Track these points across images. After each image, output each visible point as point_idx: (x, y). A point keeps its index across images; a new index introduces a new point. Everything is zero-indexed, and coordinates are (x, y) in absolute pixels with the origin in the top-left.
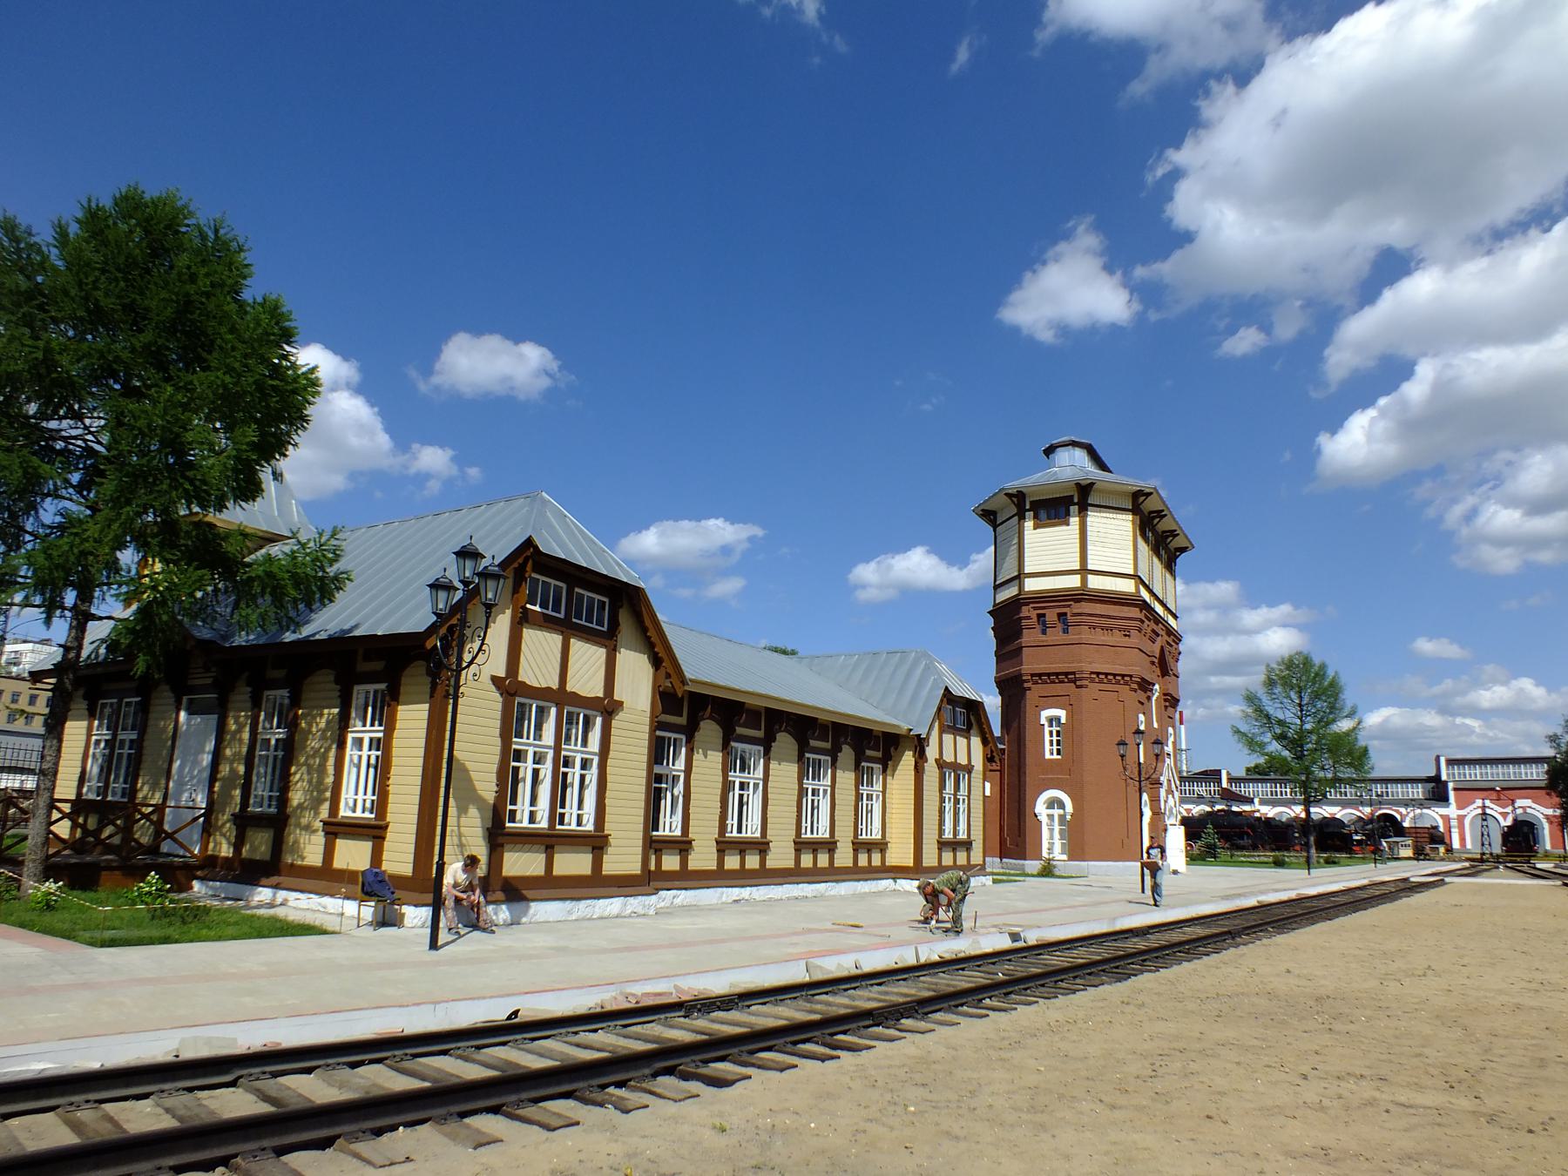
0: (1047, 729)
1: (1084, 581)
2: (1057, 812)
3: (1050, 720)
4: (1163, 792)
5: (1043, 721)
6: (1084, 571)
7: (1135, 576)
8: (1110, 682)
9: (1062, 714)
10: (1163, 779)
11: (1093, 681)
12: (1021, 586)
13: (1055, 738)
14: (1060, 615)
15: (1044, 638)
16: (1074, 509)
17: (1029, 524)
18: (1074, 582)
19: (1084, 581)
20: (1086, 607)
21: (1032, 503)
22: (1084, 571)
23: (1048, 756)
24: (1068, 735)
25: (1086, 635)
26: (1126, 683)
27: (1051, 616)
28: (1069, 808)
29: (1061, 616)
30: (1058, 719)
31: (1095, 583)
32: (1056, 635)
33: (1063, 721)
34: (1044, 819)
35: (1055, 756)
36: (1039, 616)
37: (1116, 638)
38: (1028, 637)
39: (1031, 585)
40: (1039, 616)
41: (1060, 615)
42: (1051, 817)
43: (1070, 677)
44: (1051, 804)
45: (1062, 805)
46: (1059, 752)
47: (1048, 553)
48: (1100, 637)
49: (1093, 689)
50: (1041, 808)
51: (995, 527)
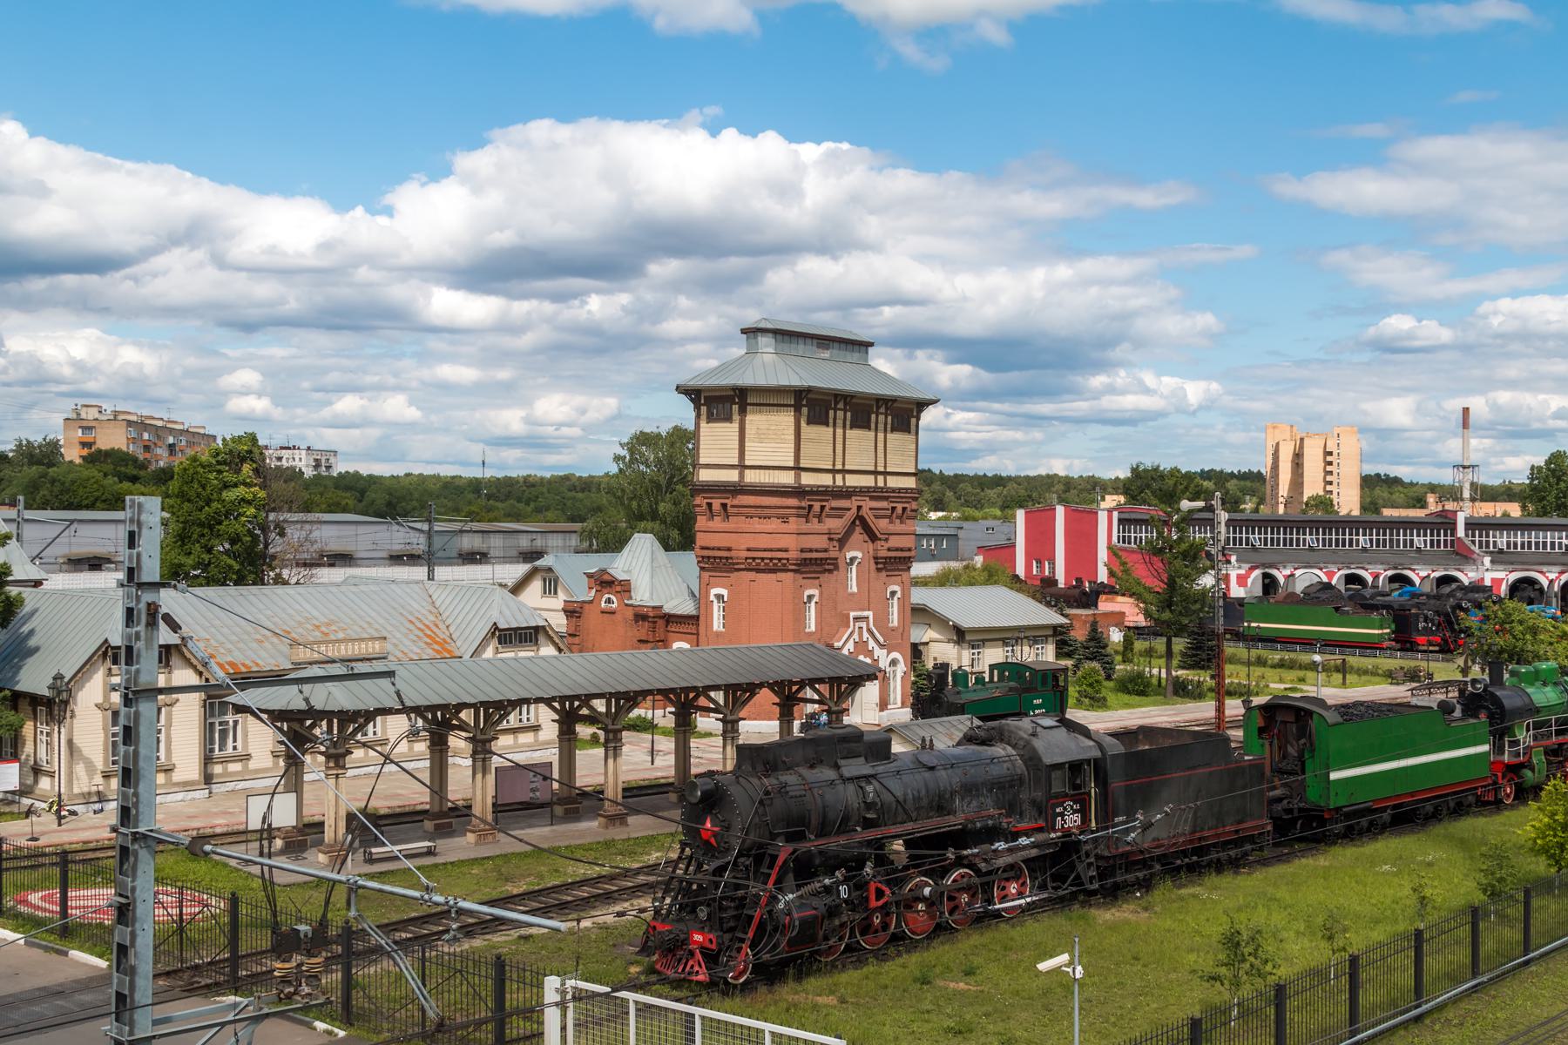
1: (742, 475)
5: (712, 598)
7: (798, 469)
9: (724, 592)
15: (711, 524)
16: (735, 408)
18: (732, 476)
19: (742, 475)
27: (716, 504)
29: (724, 506)
31: (751, 477)
32: (717, 523)
38: (701, 522)
39: (705, 476)
47: (717, 448)
48: (757, 524)
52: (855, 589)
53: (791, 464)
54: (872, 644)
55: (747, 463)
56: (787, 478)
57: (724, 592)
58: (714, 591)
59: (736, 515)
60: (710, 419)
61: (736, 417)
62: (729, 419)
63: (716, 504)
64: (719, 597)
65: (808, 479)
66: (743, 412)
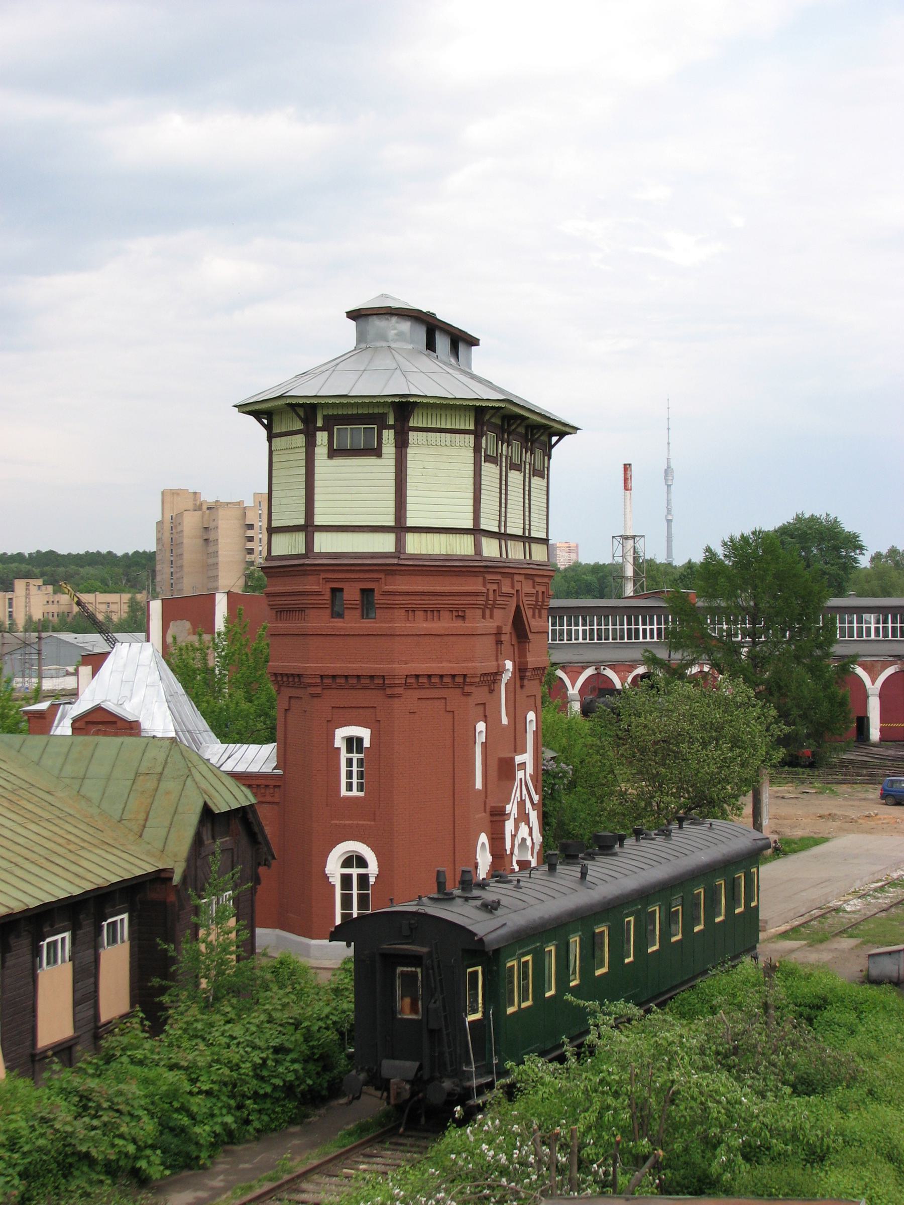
0: (344, 755)
1: (400, 543)
2: (355, 872)
3: (350, 741)
4: (509, 826)
5: (339, 743)
6: (400, 528)
8: (433, 686)
9: (364, 733)
10: (512, 809)
11: (407, 686)
12: (309, 543)
13: (355, 769)
14: (363, 591)
15: (338, 623)
16: (388, 436)
17: (321, 450)
18: (385, 544)
20: (402, 584)
21: (326, 418)
22: (400, 528)
23: (344, 792)
24: (374, 764)
25: (400, 623)
26: (457, 686)
27: (352, 593)
28: (373, 869)
29: (367, 593)
30: (360, 740)
31: (415, 545)
32: (352, 622)
33: (367, 744)
34: (336, 881)
35: (355, 793)
36: (334, 591)
37: (445, 624)
39: (325, 543)
40: (334, 591)
41: (363, 591)
42: (346, 880)
43: (378, 683)
44: (348, 862)
45: (361, 862)
46: (361, 788)
47: (352, 498)
48: (422, 624)
49: (409, 699)
50: (334, 868)
51: (270, 439)
52: (505, 721)
53: (469, 524)
54: (528, 805)
55: (410, 523)
56: (463, 546)
57: (364, 733)
58: (342, 734)
59: (390, 607)
60: (334, 453)
61: (389, 449)
62: (377, 452)
63: (352, 593)
64: (353, 743)
65: (490, 548)
66: (402, 444)
